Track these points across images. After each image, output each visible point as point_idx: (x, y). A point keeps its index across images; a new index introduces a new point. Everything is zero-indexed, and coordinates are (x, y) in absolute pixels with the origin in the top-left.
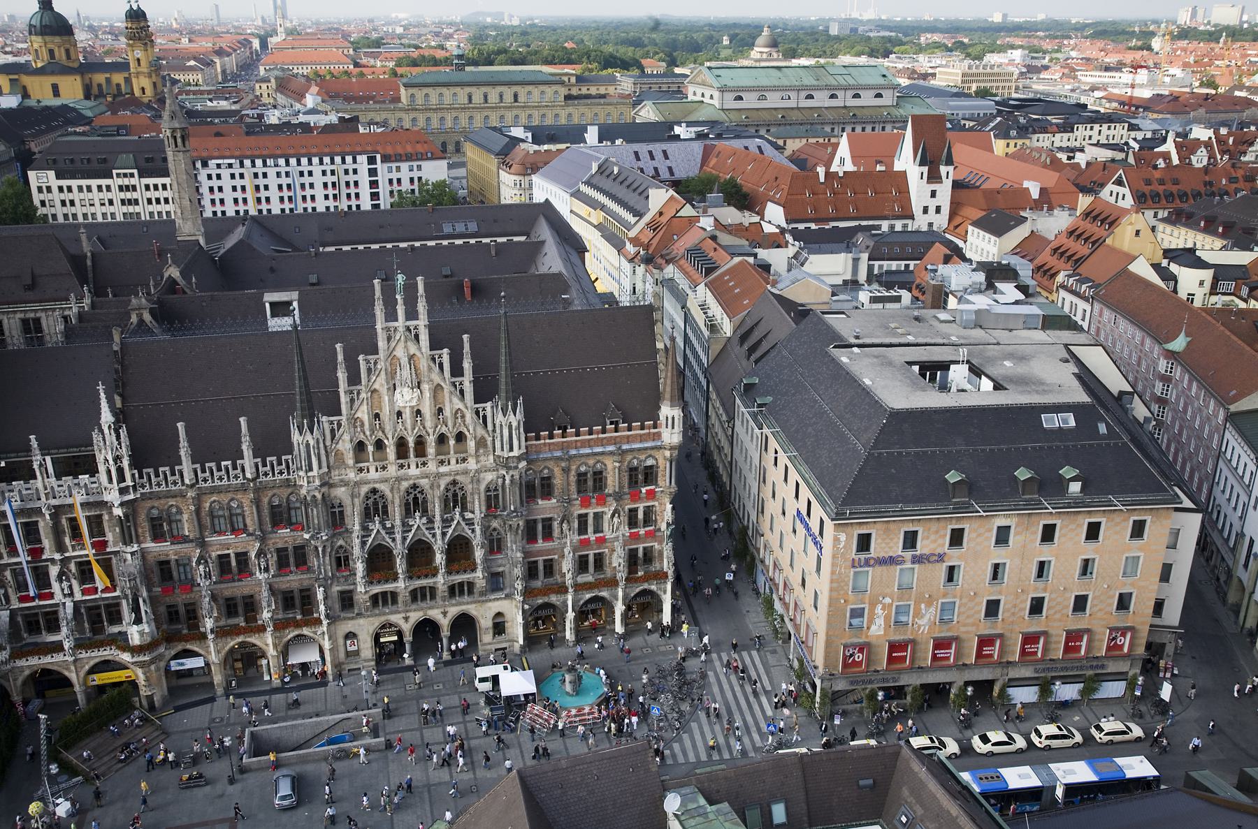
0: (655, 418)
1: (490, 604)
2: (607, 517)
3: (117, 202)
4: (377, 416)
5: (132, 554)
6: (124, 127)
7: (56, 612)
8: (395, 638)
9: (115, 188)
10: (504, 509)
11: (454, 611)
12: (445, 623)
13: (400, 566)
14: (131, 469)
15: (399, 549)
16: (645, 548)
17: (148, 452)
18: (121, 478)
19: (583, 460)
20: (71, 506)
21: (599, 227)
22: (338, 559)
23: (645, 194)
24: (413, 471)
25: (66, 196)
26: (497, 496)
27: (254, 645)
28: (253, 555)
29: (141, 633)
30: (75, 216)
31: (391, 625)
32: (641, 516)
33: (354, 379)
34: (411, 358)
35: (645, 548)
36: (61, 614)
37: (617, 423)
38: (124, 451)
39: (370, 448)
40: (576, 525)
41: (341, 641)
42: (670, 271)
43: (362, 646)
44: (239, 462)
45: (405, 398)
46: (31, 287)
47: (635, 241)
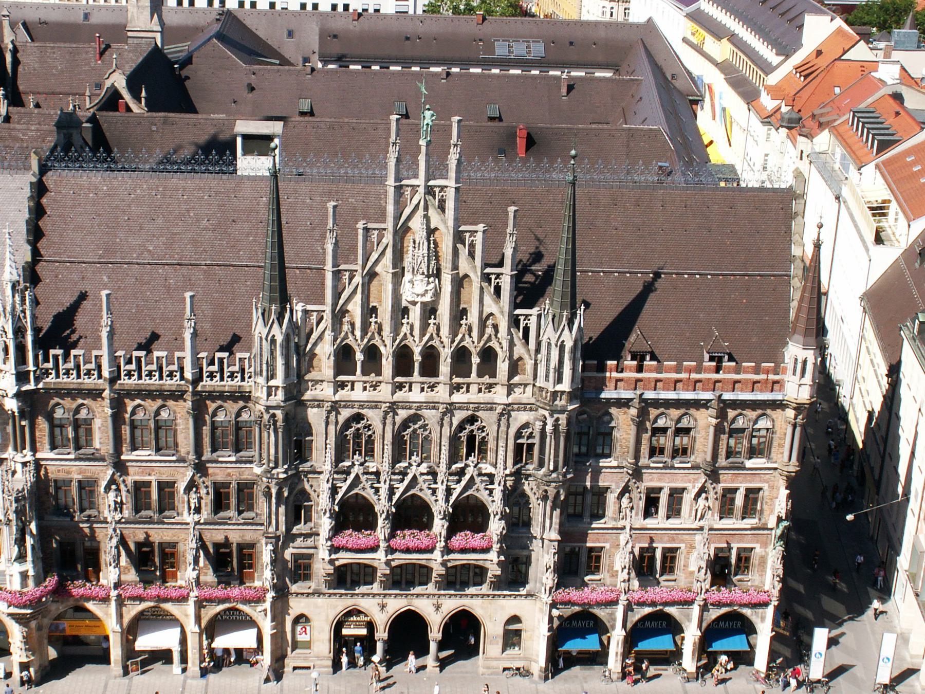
2: (688, 497)
4: (374, 310)
5: (24, 464)
8: (364, 632)
12: (435, 621)
13: (382, 528)
14: (34, 348)
21: (724, 67)
23: (797, 22)
26: (531, 447)
28: (181, 486)
29: (24, 576)
34: (431, 232)
37: (720, 360)
40: (642, 504)
42: (824, 140)
43: (316, 634)
45: (415, 289)
47: (775, 92)
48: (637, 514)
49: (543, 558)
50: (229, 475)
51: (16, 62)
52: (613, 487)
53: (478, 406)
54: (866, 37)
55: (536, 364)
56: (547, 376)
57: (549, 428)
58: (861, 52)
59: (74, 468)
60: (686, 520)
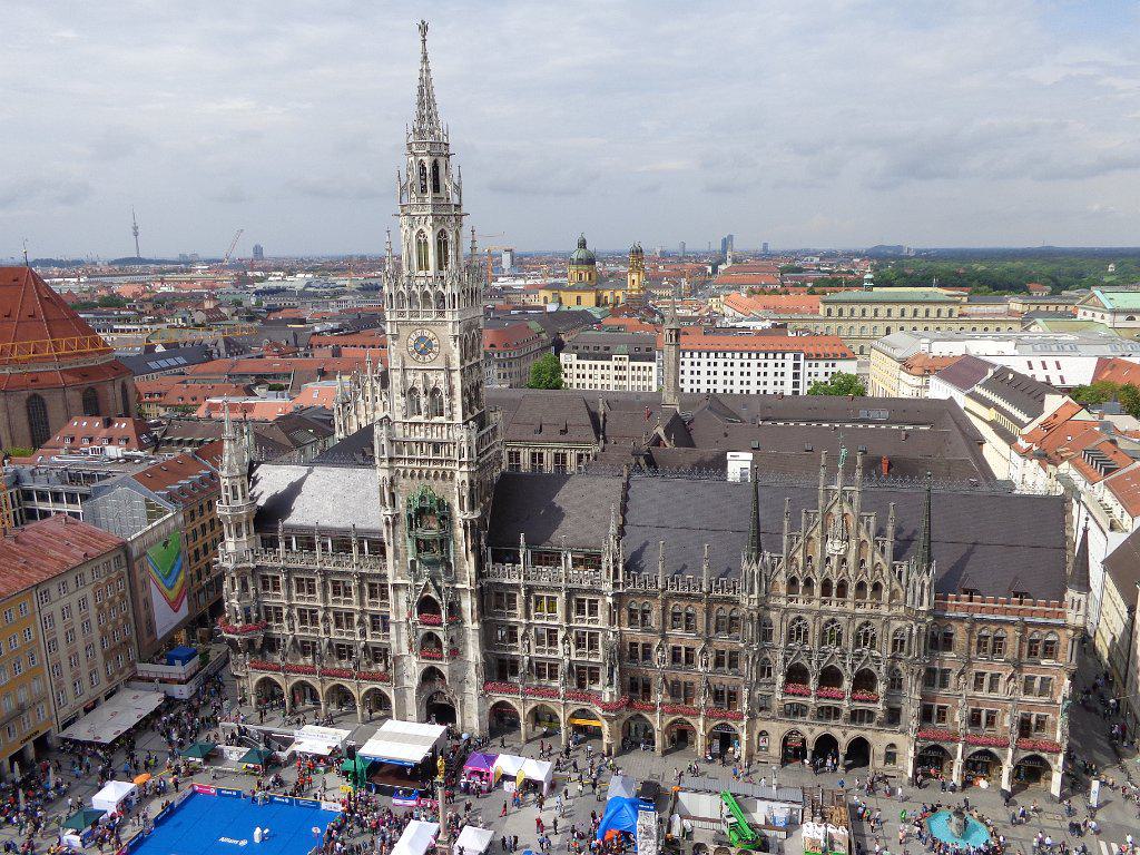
0: (1062, 599)
2: (1002, 680)
3: (612, 378)
4: (810, 558)
6: (623, 326)
9: (612, 368)
10: (909, 654)
11: (853, 733)
13: (813, 684)
15: (814, 669)
16: (1038, 716)
21: (992, 424)
22: (763, 670)
24: (833, 607)
25: (581, 371)
26: (902, 642)
29: (612, 694)
30: (584, 385)
32: (1037, 684)
33: (794, 526)
34: (844, 515)
36: (560, 668)
42: (1065, 467)
45: (834, 547)
46: (564, 432)
49: (910, 711)
51: (605, 421)
52: (954, 670)
53: (871, 615)
54: (1084, 406)
56: (914, 601)
57: (914, 632)
58: (1083, 415)
60: (1001, 692)
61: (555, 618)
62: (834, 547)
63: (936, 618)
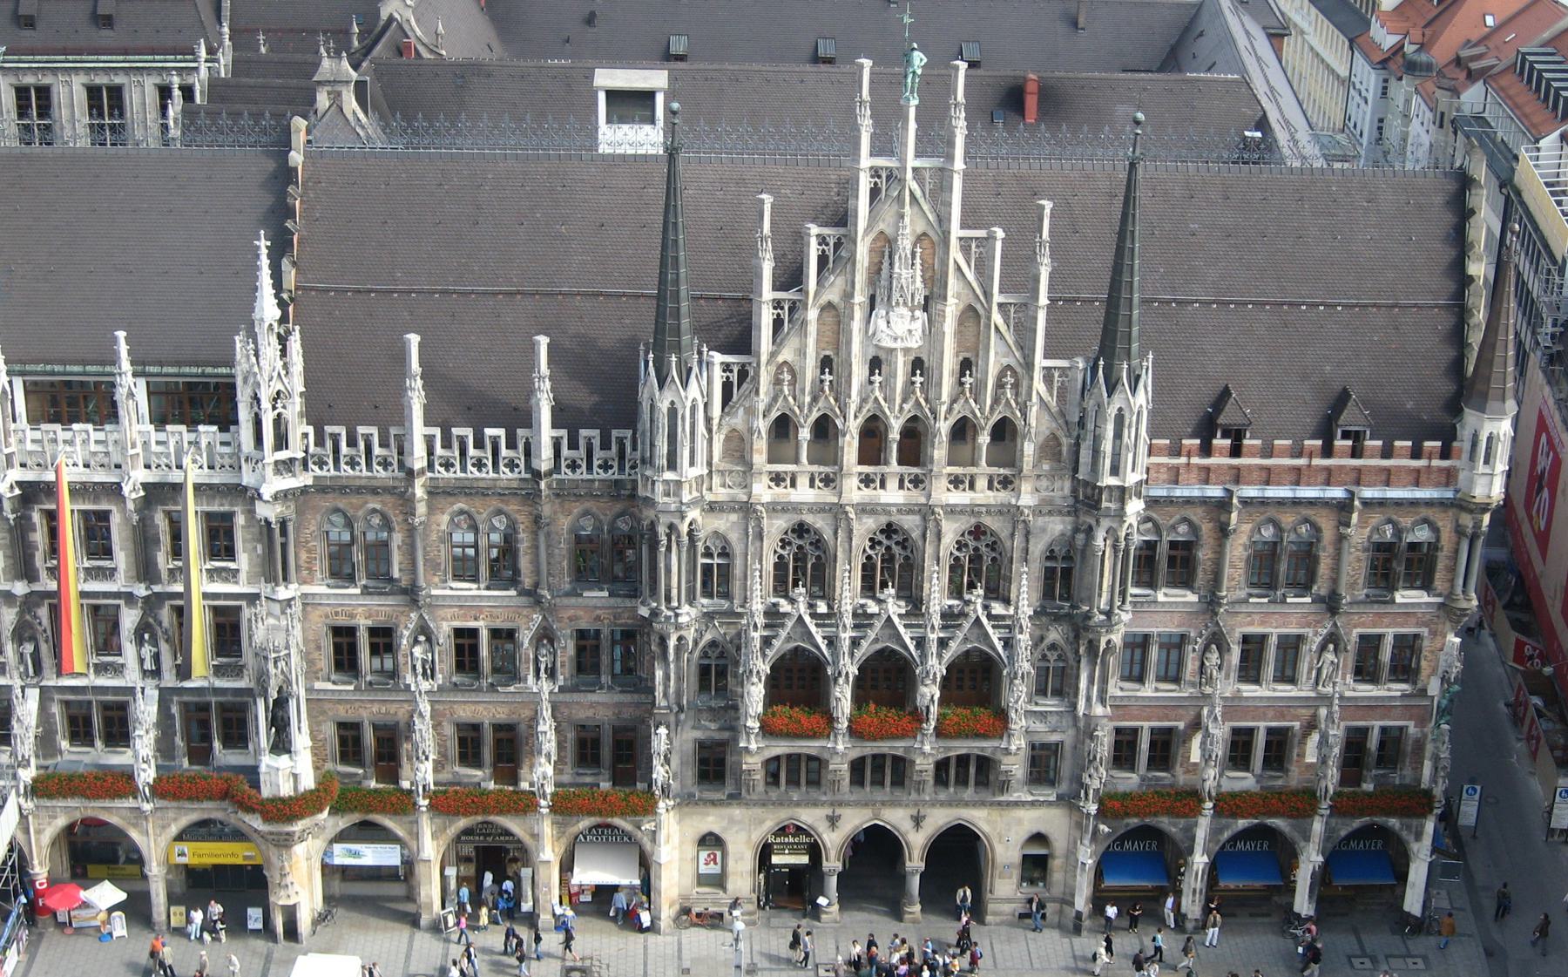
1: (1021, 813)
7: (123, 708)
8: (805, 860)
12: (916, 842)
16: (1384, 730)
17: (347, 393)
18: (281, 442)
19: (1271, 512)
20: (177, 488)
27: (507, 833)
28: (526, 638)
31: (799, 830)
32: (1386, 654)
33: (790, 277)
35: (1384, 730)
37: (1357, 437)
38: (298, 384)
39: (805, 434)
41: (691, 849)
42: (1473, 97)
44: (521, 432)
48: (1227, 676)
50: (598, 618)
55: (1077, 445)
59: (360, 610)
61: (110, 574)
62: (901, 329)
63: (1152, 503)
